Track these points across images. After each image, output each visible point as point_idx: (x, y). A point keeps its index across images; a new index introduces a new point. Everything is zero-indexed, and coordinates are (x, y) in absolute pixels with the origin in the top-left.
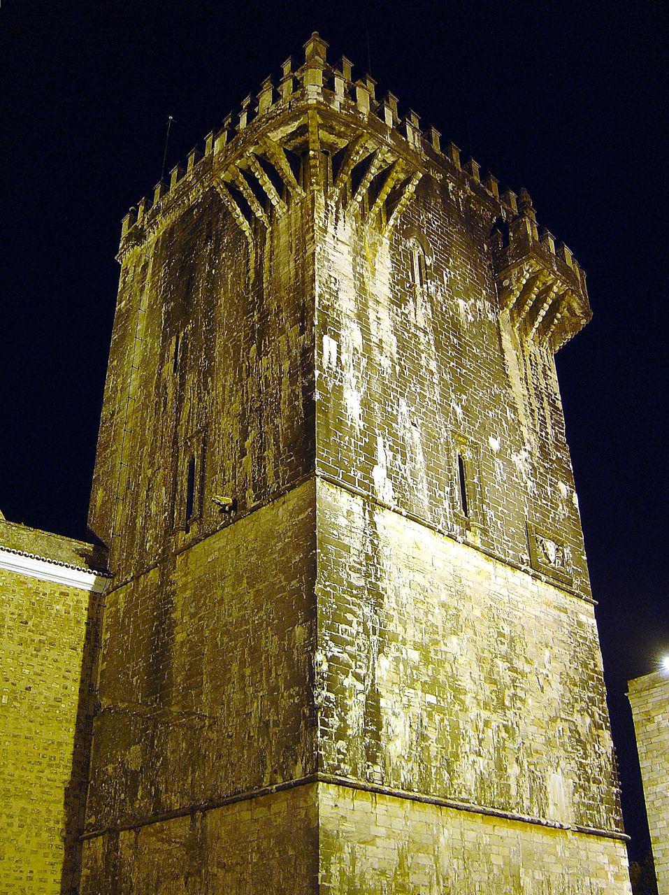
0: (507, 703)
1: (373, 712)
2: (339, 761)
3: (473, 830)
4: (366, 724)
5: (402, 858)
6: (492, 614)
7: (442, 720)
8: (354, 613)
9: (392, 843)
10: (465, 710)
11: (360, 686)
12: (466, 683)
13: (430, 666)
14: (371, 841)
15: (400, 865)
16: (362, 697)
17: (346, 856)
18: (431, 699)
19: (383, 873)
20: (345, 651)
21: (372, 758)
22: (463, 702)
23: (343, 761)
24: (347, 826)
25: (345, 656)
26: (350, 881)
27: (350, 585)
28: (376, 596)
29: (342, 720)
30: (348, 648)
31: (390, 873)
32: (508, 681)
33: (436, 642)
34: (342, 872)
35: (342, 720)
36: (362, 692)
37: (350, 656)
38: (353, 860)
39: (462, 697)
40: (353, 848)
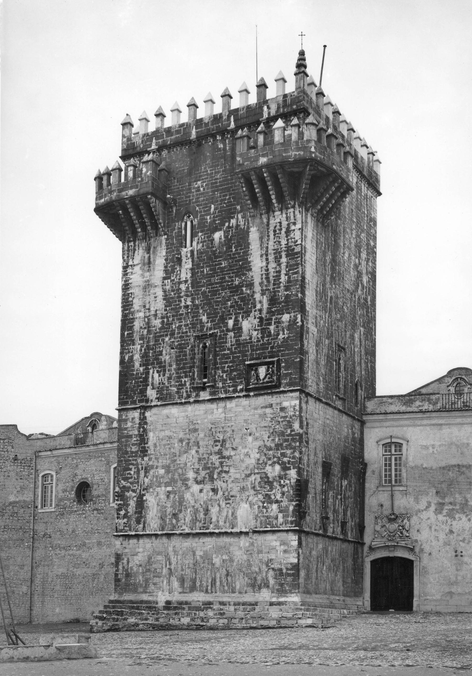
0: (215, 476)
1: (141, 504)
2: (124, 527)
4: (136, 509)
5: (150, 558)
6: (211, 433)
7: (175, 497)
8: (133, 464)
9: (146, 554)
10: (188, 487)
11: (134, 494)
12: (191, 475)
13: (170, 474)
14: (136, 554)
15: (148, 562)
16: (135, 499)
17: (125, 561)
18: (169, 489)
19: (141, 566)
20: (128, 482)
21: (138, 522)
22: (187, 485)
23: (126, 526)
24: (126, 551)
25: (129, 484)
26: (127, 570)
27: (132, 452)
28: (144, 452)
29: (126, 510)
30: (130, 480)
31: (143, 565)
32: (217, 464)
33: (175, 461)
34: (123, 567)
35: (126, 510)
36: (135, 496)
37: (131, 483)
38: (128, 562)
39: (187, 483)
40: (128, 559)
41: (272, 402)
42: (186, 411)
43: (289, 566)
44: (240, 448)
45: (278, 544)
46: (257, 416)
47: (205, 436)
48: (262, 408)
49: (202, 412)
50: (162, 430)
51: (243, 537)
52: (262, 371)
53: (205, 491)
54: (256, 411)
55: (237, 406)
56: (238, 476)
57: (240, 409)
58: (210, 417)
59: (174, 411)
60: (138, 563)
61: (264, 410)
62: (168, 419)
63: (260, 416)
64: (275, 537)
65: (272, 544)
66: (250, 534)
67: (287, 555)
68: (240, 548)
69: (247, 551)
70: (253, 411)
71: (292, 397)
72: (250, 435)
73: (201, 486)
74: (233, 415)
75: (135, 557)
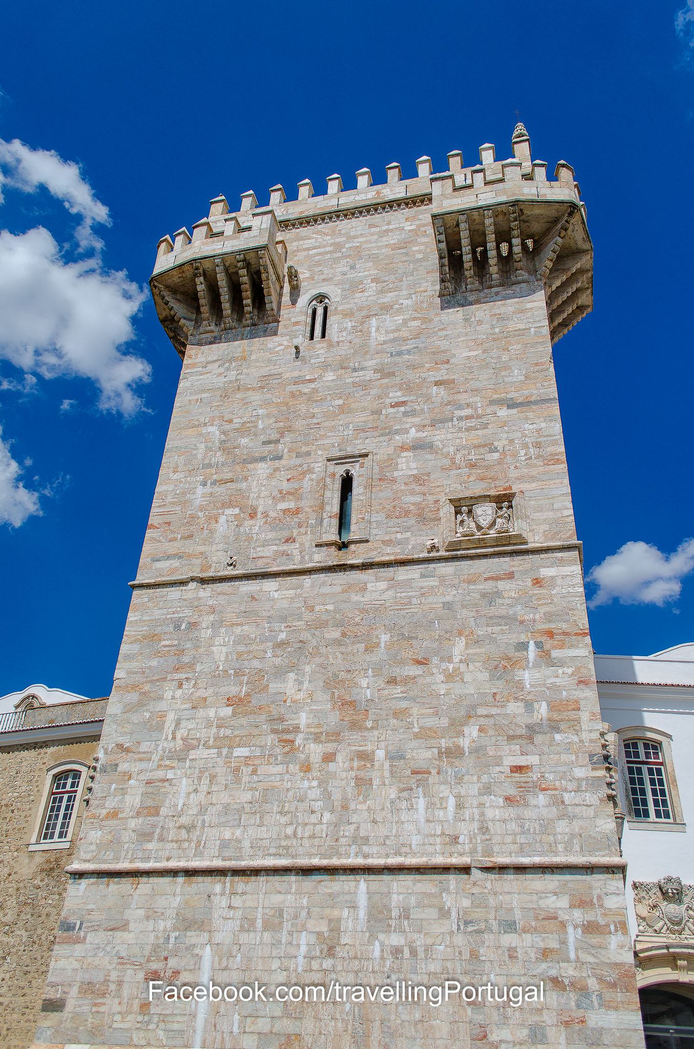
3: (280, 892)
12: (303, 719)
14: (124, 927)
41: (514, 569)
42: (300, 587)
43: (611, 976)
44: (435, 660)
45: (564, 902)
46: (477, 596)
47: (344, 634)
48: (486, 579)
49: (338, 589)
50: (238, 625)
51: (452, 880)
52: (485, 512)
53: (339, 758)
54: (473, 587)
55: (423, 576)
56: (431, 722)
57: (433, 582)
58: (355, 598)
59: (269, 585)
60: (123, 954)
61: (491, 583)
62: (255, 603)
63: (484, 595)
64: (552, 881)
65: (543, 904)
66: (476, 874)
67: (595, 940)
68: (444, 913)
69: (466, 923)
70: (465, 585)
71: (561, 560)
72: (460, 634)
73: (330, 747)
74: (414, 593)
75: (118, 934)
